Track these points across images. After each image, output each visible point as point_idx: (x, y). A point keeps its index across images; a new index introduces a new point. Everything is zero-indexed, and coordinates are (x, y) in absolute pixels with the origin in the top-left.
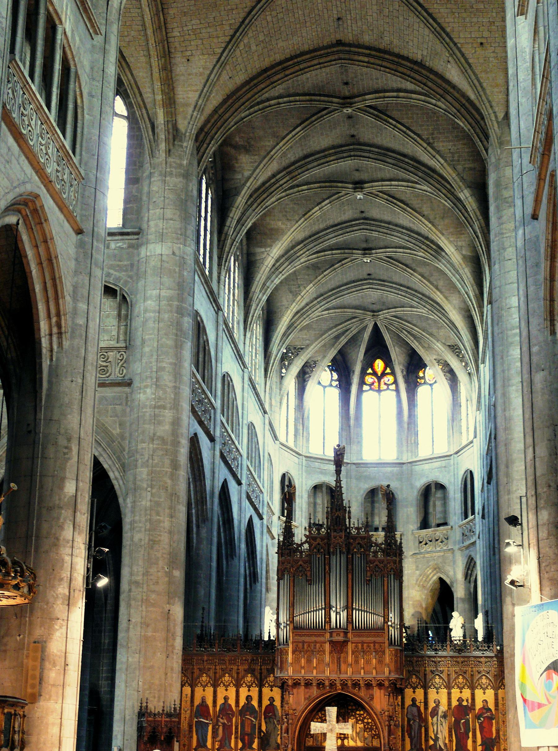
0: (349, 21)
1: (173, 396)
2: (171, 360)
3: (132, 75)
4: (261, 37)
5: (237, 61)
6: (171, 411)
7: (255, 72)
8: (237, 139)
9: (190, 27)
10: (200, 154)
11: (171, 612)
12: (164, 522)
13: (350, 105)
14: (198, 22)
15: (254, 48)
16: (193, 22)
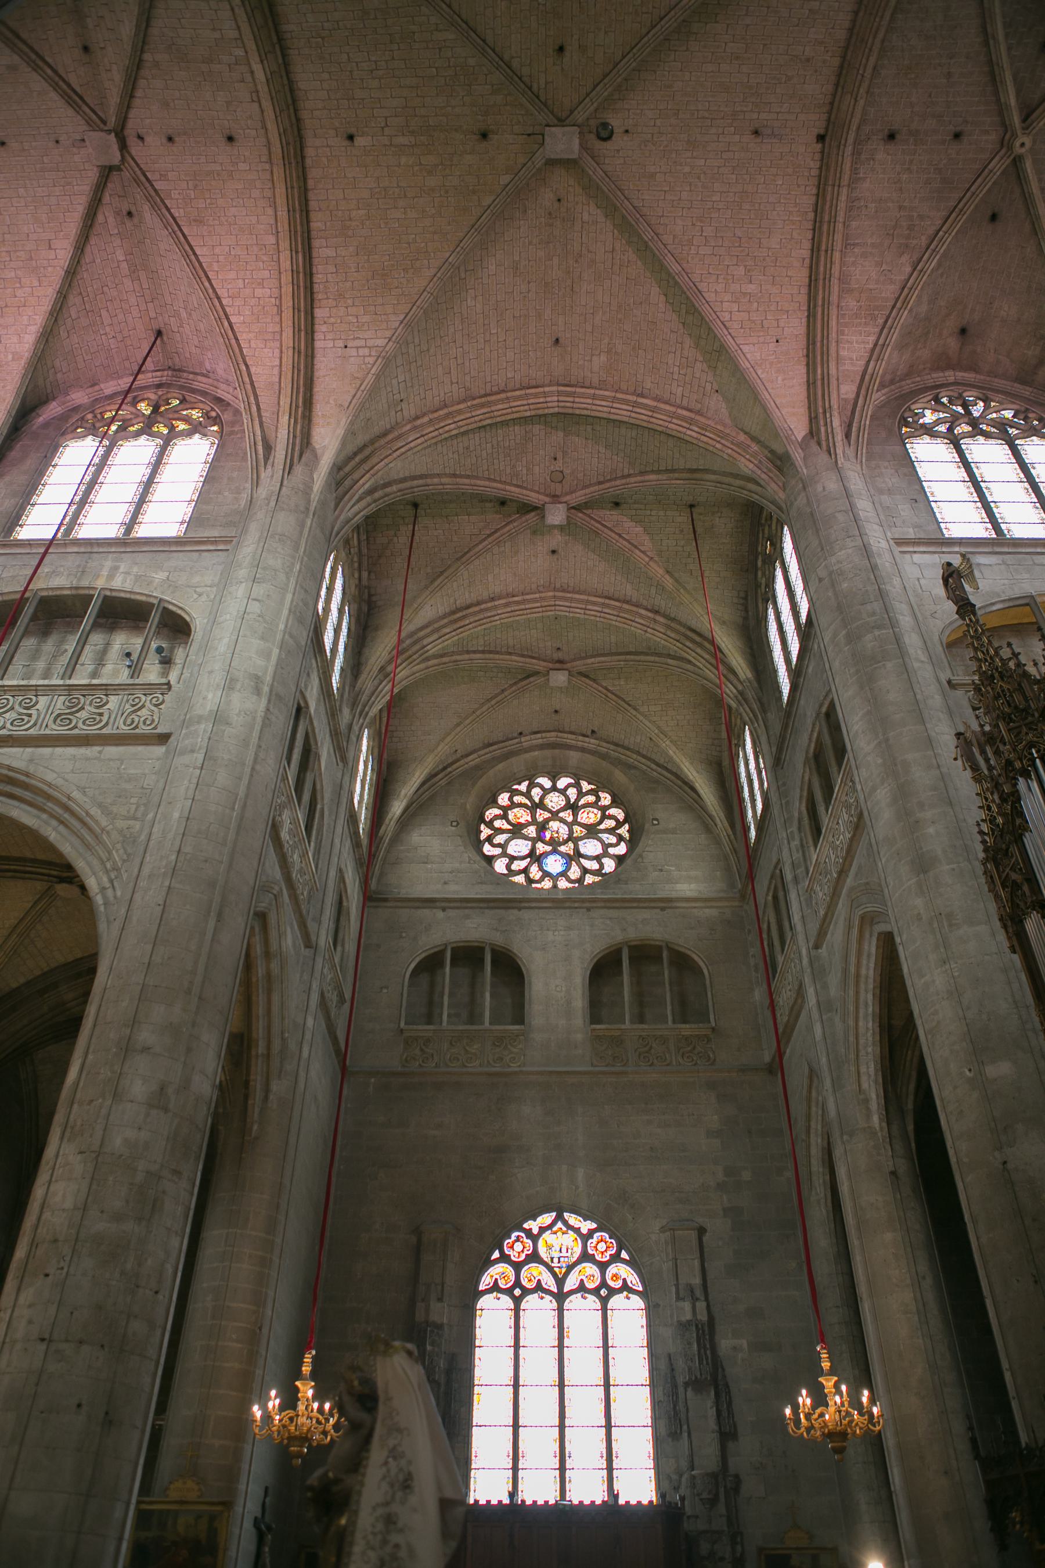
0: (763, 116)
1: (880, 761)
2: (860, 714)
3: (714, 473)
4: (741, 271)
5: (754, 322)
6: (886, 785)
7: (803, 298)
8: (1030, 353)
9: (676, 369)
10: (824, 443)
11: (1009, 1166)
12: (934, 981)
13: (1014, 136)
14: (672, 355)
15: (751, 288)
16: (670, 362)
